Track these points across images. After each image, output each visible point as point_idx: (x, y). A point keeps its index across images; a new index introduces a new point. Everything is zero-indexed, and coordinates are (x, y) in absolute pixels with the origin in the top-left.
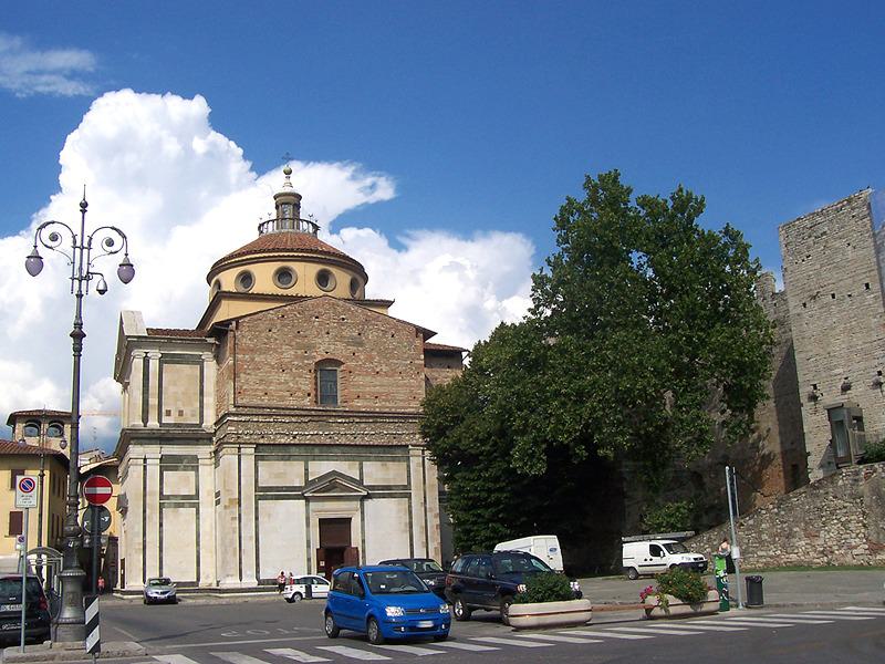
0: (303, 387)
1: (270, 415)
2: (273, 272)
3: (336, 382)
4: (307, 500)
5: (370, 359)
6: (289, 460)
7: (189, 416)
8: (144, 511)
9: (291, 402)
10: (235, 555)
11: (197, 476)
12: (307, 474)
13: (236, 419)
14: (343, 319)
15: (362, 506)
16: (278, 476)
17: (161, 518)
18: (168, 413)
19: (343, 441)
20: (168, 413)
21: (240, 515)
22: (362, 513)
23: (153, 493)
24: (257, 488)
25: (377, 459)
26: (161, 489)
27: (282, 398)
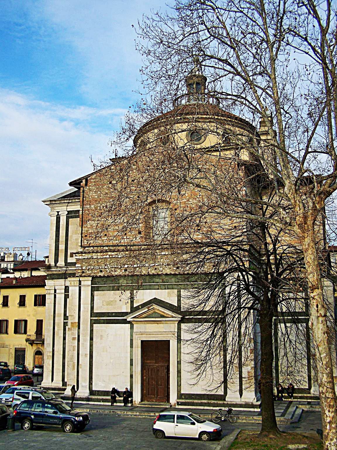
1: (106, 251)
4: (129, 322)
10: (74, 369)
13: (81, 257)
15: (179, 329)
16: (109, 303)
18: (72, 255)
21: (79, 336)
24: (92, 314)
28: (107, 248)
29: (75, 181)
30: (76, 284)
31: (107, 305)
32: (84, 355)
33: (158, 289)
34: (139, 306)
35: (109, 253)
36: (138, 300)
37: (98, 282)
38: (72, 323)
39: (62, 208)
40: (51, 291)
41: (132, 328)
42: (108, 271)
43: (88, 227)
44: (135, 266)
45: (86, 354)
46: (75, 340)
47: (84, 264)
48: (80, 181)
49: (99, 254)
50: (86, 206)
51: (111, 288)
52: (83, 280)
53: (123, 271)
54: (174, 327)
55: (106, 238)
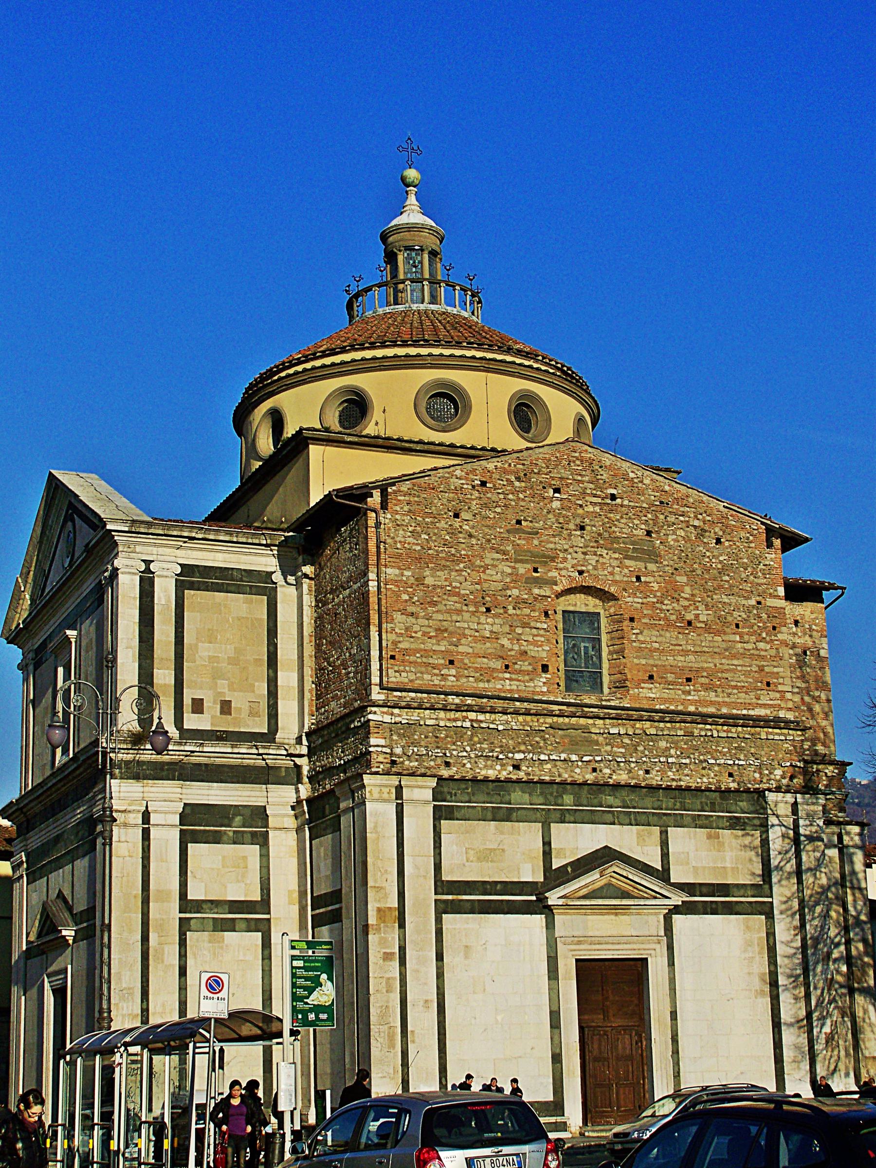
0: (533, 650)
2: (376, 414)
3: (599, 640)
5: (672, 591)
6: (508, 820)
7: (244, 714)
8: (145, 938)
9: (506, 684)
11: (265, 856)
12: (547, 854)
14: (613, 497)
16: (485, 856)
17: (183, 956)
19: (622, 777)
20: (198, 706)
21: (402, 949)
22: (670, 948)
23: (164, 896)
25: (697, 823)
26: (183, 885)
27: (487, 674)
28: (457, 700)
29: (351, 488)
30: (386, 796)
31: (479, 859)
32: (422, 1003)
33: (613, 823)
34: (566, 866)
35: (472, 715)
36: (560, 851)
37: (450, 793)
38: (379, 910)
39: (161, 550)
40: (131, 815)
41: (550, 925)
42: (468, 766)
43: (397, 630)
44: (543, 757)
45: (426, 1001)
46: (391, 960)
47: (395, 737)
48: (365, 491)
49: (442, 714)
50: (389, 571)
51: (489, 815)
52: (407, 786)
53: (511, 768)
54: (656, 924)
55: (453, 672)
